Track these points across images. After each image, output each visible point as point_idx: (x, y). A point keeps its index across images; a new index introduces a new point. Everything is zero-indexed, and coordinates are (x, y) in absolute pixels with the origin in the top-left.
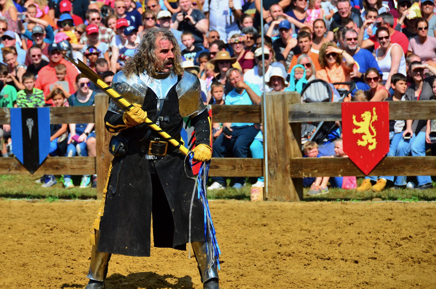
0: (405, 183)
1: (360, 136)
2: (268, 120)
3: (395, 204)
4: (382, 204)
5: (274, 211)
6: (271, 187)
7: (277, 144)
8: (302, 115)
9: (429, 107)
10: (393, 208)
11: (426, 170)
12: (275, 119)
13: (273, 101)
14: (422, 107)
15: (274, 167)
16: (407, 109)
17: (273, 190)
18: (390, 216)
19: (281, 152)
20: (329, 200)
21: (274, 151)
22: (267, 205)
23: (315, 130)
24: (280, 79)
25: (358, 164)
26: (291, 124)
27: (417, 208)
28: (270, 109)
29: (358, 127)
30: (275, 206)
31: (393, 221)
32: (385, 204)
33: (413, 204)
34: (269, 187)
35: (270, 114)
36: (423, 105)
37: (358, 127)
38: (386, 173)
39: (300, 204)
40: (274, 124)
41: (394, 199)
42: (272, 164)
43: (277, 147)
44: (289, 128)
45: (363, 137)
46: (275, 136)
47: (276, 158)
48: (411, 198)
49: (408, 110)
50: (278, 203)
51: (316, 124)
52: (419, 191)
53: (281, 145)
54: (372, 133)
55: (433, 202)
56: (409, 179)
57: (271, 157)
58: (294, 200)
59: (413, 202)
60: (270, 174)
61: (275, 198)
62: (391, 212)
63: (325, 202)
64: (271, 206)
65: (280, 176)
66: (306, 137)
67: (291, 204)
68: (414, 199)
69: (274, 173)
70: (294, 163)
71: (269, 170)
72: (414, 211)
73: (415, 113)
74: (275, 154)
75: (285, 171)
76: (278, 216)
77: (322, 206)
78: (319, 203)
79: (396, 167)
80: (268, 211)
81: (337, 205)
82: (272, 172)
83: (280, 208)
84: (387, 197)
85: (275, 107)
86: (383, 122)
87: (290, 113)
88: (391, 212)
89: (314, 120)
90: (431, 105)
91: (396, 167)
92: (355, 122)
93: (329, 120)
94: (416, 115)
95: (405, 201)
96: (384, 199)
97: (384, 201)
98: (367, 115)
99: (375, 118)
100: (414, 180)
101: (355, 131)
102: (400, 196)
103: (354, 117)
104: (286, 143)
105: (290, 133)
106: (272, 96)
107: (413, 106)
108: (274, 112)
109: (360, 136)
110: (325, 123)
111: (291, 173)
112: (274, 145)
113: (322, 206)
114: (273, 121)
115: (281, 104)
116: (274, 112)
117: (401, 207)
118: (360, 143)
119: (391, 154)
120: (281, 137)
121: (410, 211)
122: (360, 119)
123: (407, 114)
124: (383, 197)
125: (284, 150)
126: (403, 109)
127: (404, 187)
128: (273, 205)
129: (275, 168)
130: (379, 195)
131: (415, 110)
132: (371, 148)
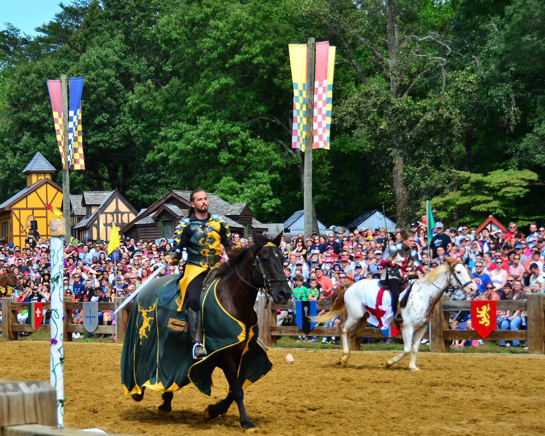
0: (504, 344)
1: (480, 319)
8: (450, 307)
17: (434, 347)
20: (463, 352)
23: (457, 315)
25: (479, 333)
26: (445, 312)
29: (479, 314)
37: (479, 314)
39: (447, 354)
44: (443, 314)
45: (482, 319)
50: (435, 353)
51: (457, 312)
52: (513, 348)
53: (438, 323)
54: (487, 317)
56: (507, 342)
58: (445, 352)
60: (432, 338)
63: (461, 354)
65: (437, 339)
66: (452, 318)
67: (444, 354)
70: (445, 332)
75: (441, 336)
77: (459, 355)
78: (457, 354)
81: (468, 355)
87: (443, 306)
89: (456, 310)
92: (478, 311)
93: (464, 310)
98: (484, 308)
99: (489, 309)
100: (511, 342)
101: (478, 316)
103: (477, 309)
104: (441, 322)
105: (443, 317)
109: (480, 319)
110: (462, 311)
111: (443, 338)
113: (459, 355)
118: (480, 322)
120: (438, 319)
122: (481, 310)
125: (440, 325)
127: (504, 346)
132: (487, 325)
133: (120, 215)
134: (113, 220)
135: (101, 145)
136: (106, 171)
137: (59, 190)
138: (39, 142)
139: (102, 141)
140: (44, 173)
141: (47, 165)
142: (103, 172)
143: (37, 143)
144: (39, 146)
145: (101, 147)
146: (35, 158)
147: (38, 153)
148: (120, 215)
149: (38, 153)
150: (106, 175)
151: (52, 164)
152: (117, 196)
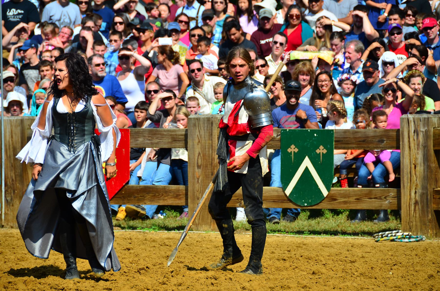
2: (5, 146)
3: (134, 233)
4: (121, 233)
5: (10, 239)
6: (8, 214)
7: (15, 170)
9: (171, 135)
10: (132, 237)
11: (166, 200)
12: (13, 144)
13: (11, 126)
14: (163, 135)
15: (11, 193)
16: (149, 137)
17: (10, 218)
18: (129, 246)
19: (18, 179)
21: (12, 177)
22: (3, 232)
24: (19, 104)
27: (157, 238)
28: (8, 134)
30: (11, 233)
31: (131, 251)
32: (125, 233)
33: (153, 234)
34: (5, 214)
35: (8, 139)
36: (165, 133)
38: (125, 201)
40: (12, 150)
41: (134, 228)
42: (9, 190)
43: (15, 173)
46: (12, 161)
47: (13, 184)
48: (151, 227)
49: (150, 138)
55: (173, 231)
57: (8, 183)
59: (152, 231)
60: (6, 201)
61: (12, 225)
62: (129, 241)
64: (7, 234)
68: (154, 229)
69: (11, 199)
71: (5, 197)
72: (154, 241)
73: (156, 141)
74: (13, 180)
76: (14, 244)
79: (136, 195)
80: (4, 239)
82: (9, 199)
83: (16, 236)
84: (126, 226)
85: (13, 132)
86: (124, 150)
88: (129, 241)
90: (173, 133)
91: (136, 195)
94: (157, 143)
95: (144, 230)
96: (123, 228)
97: (124, 230)
102: (139, 226)
106: (10, 121)
107: (155, 134)
108: (12, 137)
112: (11, 171)
114: (11, 147)
115: (19, 128)
116: (12, 137)
117: (140, 237)
119: (133, 182)
121: (149, 241)
123: (149, 142)
124: (122, 226)
126: (145, 136)
128: (9, 232)
129: (12, 194)
130: (118, 224)
131: (157, 138)
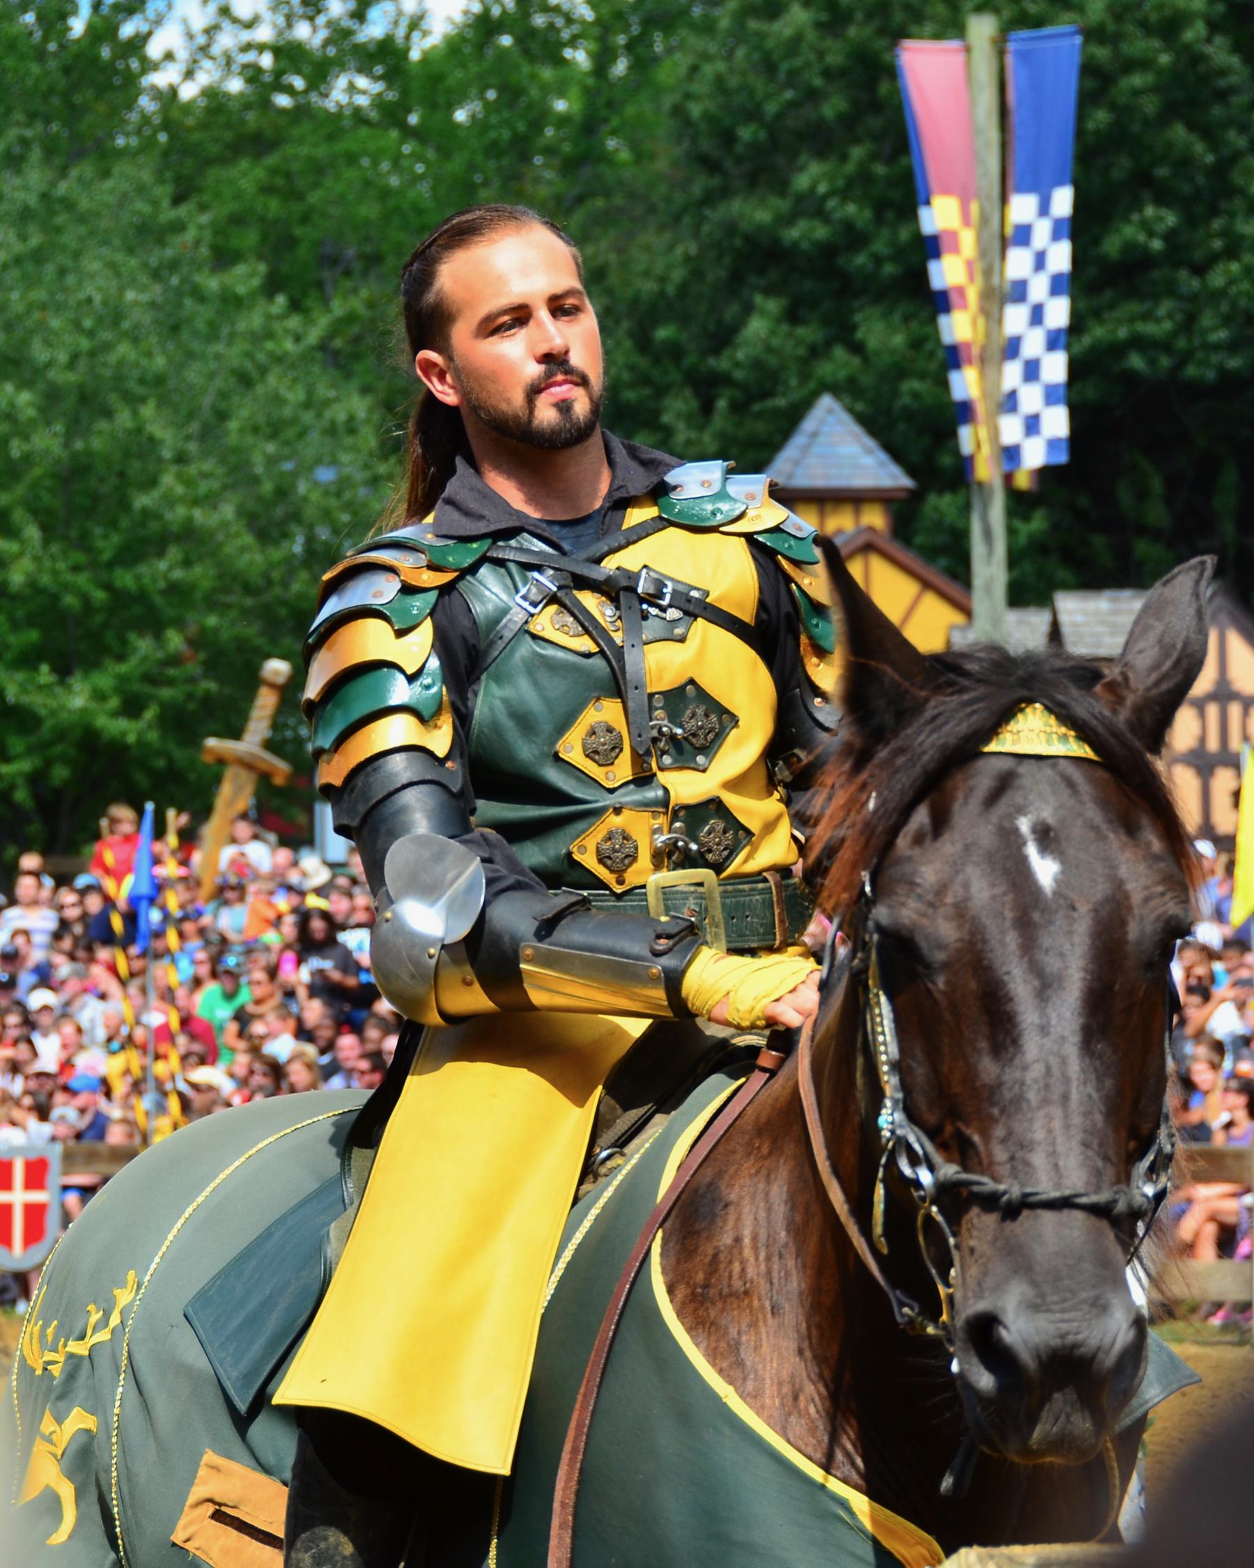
133: (1235, 710)
134: (1203, 740)
135: (1136, 361)
136: (1157, 485)
137: (926, 585)
138: (828, 344)
139: (1138, 343)
140: (855, 499)
141: (868, 461)
142: (1142, 495)
143: (816, 352)
144: (825, 369)
145: (1131, 377)
146: (809, 424)
147: (826, 402)
148: (1235, 710)
149: (826, 402)
150: (1157, 514)
151: (895, 452)
152: (1223, 617)
